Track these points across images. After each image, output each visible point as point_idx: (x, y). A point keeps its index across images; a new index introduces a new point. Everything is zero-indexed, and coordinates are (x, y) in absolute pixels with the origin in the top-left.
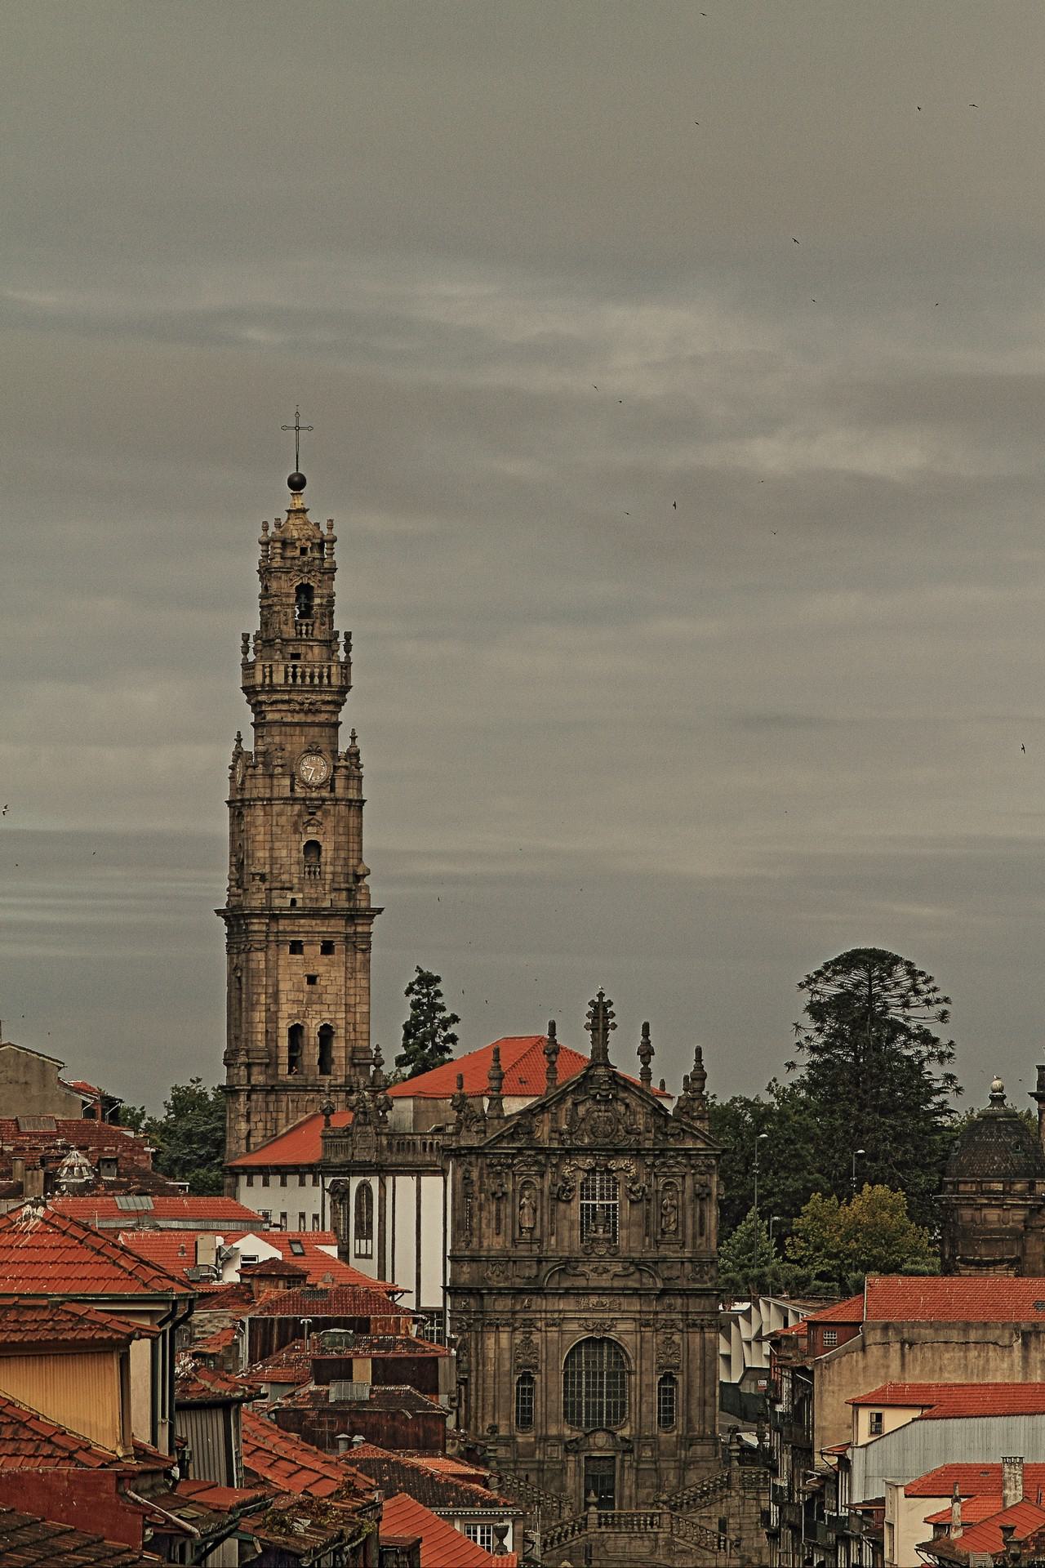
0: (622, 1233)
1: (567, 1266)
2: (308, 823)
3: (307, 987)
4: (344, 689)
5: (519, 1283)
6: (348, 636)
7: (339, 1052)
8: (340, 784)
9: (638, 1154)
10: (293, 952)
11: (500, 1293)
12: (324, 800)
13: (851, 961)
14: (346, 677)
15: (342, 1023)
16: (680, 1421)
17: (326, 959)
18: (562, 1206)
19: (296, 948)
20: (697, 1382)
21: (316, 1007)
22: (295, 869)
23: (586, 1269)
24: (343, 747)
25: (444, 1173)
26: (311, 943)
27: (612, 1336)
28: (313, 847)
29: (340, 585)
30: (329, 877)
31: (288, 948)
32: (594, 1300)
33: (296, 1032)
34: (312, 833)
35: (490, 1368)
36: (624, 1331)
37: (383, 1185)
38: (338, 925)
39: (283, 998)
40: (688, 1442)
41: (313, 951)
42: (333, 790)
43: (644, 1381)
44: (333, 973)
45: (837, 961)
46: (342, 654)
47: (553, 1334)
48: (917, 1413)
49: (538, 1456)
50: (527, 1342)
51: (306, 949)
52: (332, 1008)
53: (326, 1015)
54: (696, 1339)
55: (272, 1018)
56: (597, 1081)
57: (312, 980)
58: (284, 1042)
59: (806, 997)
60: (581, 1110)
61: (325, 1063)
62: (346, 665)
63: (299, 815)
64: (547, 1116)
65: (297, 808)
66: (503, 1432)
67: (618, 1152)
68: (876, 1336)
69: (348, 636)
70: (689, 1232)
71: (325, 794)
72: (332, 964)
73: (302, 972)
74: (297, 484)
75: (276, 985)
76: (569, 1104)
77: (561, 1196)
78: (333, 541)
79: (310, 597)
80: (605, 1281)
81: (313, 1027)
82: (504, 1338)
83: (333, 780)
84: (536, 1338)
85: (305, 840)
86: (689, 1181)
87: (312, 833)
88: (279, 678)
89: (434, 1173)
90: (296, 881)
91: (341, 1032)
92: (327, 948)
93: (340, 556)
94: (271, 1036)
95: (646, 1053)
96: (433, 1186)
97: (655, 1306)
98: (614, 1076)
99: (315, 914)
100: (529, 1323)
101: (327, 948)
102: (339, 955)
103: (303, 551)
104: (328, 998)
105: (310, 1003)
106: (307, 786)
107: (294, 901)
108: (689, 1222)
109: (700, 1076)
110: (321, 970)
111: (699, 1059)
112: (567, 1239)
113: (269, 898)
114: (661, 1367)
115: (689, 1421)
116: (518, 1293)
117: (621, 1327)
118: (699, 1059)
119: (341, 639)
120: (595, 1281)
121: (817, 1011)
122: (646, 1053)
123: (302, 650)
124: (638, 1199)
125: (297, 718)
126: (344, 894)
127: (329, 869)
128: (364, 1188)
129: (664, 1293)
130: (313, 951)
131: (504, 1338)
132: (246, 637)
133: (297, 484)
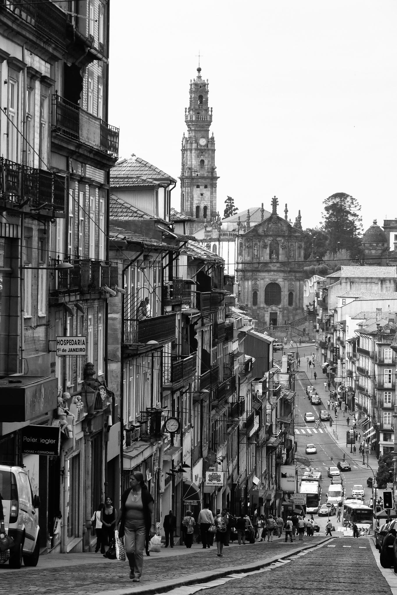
0: (280, 256)
1: (266, 264)
2: (201, 155)
4: (211, 121)
5: (254, 269)
6: (212, 108)
7: (209, 212)
8: (209, 145)
9: (284, 237)
10: (197, 187)
11: (249, 271)
12: (205, 149)
13: (335, 196)
14: (211, 119)
15: (209, 205)
16: (294, 304)
17: (205, 189)
18: (265, 250)
19: (198, 187)
20: (298, 294)
22: (198, 167)
23: (270, 265)
24: (210, 136)
25: (235, 241)
27: (277, 282)
28: (202, 162)
29: (209, 96)
32: (272, 273)
33: (198, 208)
34: (202, 158)
35: (246, 290)
36: (280, 281)
37: (219, 244)
38: (208, 181)
39: (195, 199)
40: (296, 309)
42: (207, 147)
43: (285, 293)
44: (207, 193)
45: (332, 196)
46: (210, 113)
47: (262, 282)
48: (354, 299)
49: (258, 312)
50: (256, 284)
54: (298, 283)
55: (192, 204)
56: (274, 218)
57: (202, 195)
58: (195, 210)
59: (325, 205)
60: (270, 225)
61: (205, 216)
62: (211, 116)
64: (261, 227)
66: (249, 306)
67: (279, 236)
68: (344, 281)
69: (212, 108)
70: (297, 256)
72: (207, 191)
74: (199, 70)
75: (193, 196)
76: (267, 224)
77: (265, 247)
78: (208, 84)
79: (202, 99)
80: (275, 268)
81: (202, 206)
82: (250, 282)
84: (258, 282)
86: (297, 244)
87: (202, 158)
88: (194, 119)
89: (233, 241)
91: (209, 208)
92: (206, 187)
93: (210, 88)
94: (191, 208)
95: (286, 211)
96: (232, 244)
97: (288, 275)
98: (278, 218)
99: (203, 178)
100: (256, 279)
102: (209, 189)
103: (201, 87)
104: (206, 199)
105: (201, 200)
106: (201, 146)
107: (197, 175)
108: (297, 253)
109: (300, 217)
110: (204, 192)
111: (299, 213)
112: (265, 257)
113: (191, 174)
114: (289, 290)
115: (296, 303)
116: (252, 271)
117: (279, 280)
118: (299, 213)
119: (210, 109)
120: (273, 268)
121: (327, 209)
122: (286, 211)
123: (200, 112)
124: (284, 248)
125: (199, 129)
126: (210, 173)
127: (206, 167)
128: (215, 246)
129: (290, 272)
131: (250, 282)
132: (186, 109)
133: (199, 70)
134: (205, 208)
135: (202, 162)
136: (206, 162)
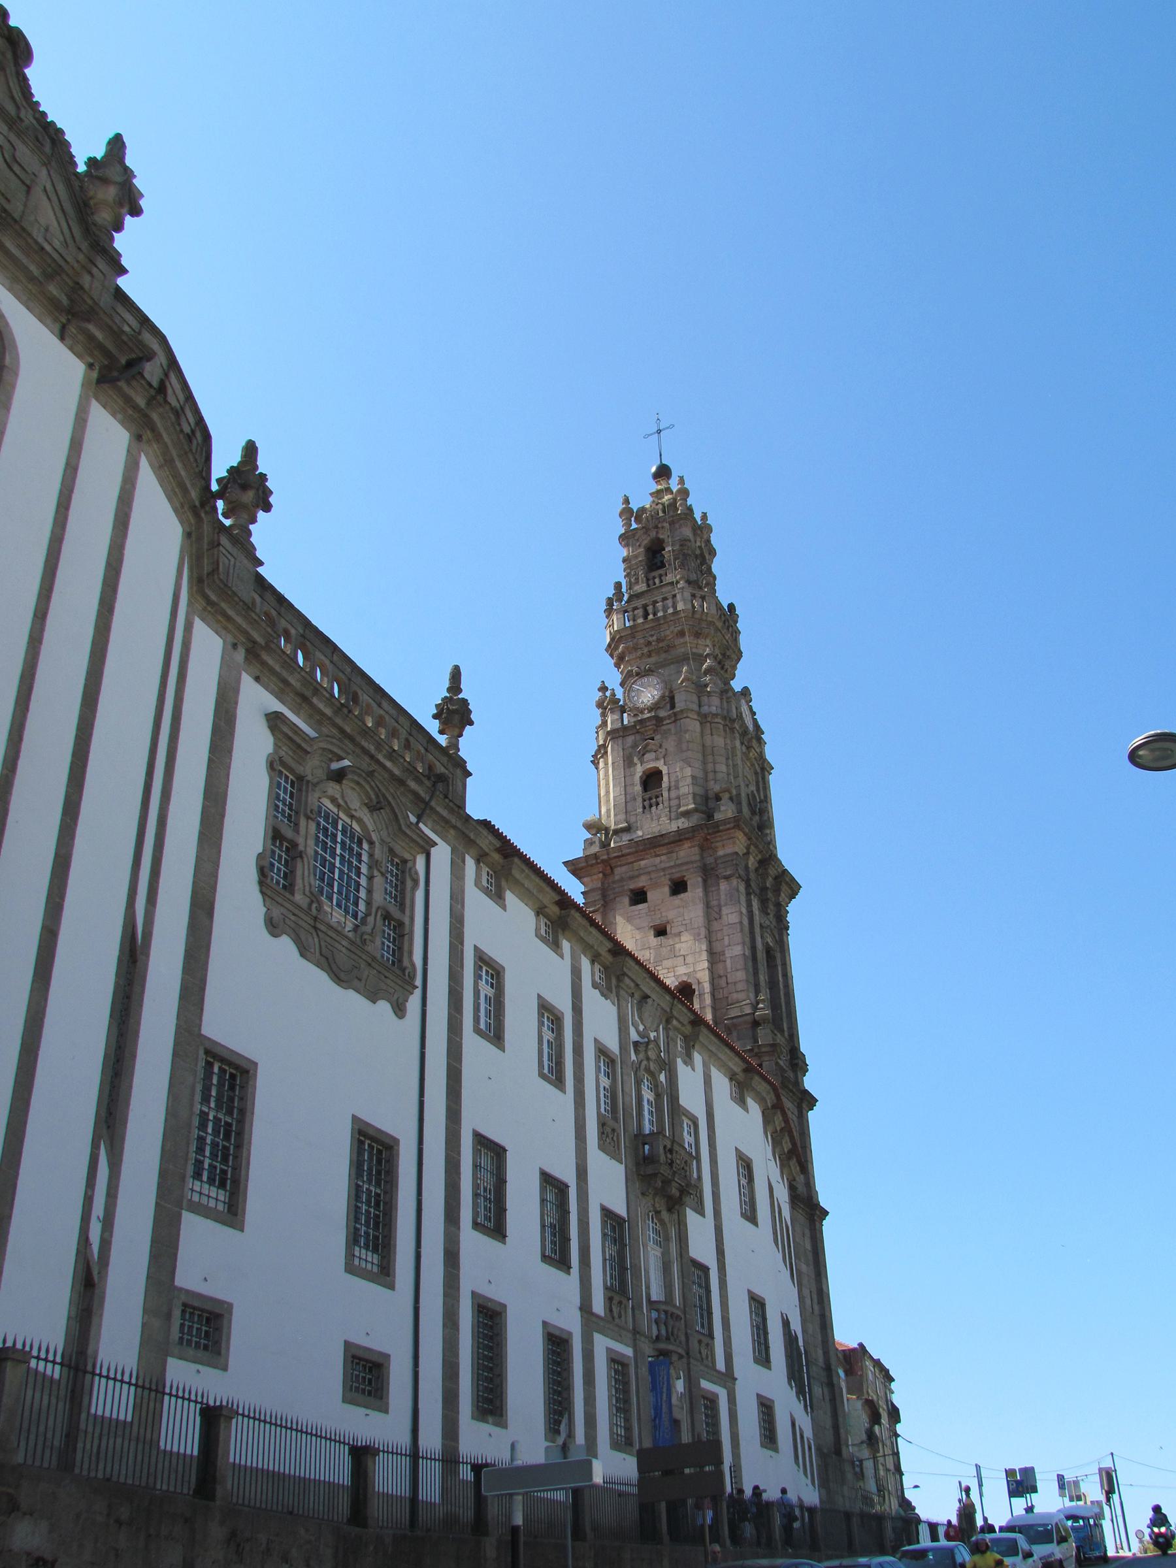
3: (653, 941)
15: (704, 976)
19: (639, 897)
21: (667, 963)
26: (656, 885)
28: (652, 780)
31: (626, 900)
38: (688, 852)
41: (659, 895)
42: (673, 706)
51: (649, 895)
52: (689, 959)
53: (682, 970)
63: (635, 746)
65: (630, 740)
71: (662, 713)
83: (672, 698)
85: (639, 770)
92: (678, 887)
102: (695, 892)
110: (671, 915)
130: (659, 895)
133: (663, 472)
135: (652, 780)
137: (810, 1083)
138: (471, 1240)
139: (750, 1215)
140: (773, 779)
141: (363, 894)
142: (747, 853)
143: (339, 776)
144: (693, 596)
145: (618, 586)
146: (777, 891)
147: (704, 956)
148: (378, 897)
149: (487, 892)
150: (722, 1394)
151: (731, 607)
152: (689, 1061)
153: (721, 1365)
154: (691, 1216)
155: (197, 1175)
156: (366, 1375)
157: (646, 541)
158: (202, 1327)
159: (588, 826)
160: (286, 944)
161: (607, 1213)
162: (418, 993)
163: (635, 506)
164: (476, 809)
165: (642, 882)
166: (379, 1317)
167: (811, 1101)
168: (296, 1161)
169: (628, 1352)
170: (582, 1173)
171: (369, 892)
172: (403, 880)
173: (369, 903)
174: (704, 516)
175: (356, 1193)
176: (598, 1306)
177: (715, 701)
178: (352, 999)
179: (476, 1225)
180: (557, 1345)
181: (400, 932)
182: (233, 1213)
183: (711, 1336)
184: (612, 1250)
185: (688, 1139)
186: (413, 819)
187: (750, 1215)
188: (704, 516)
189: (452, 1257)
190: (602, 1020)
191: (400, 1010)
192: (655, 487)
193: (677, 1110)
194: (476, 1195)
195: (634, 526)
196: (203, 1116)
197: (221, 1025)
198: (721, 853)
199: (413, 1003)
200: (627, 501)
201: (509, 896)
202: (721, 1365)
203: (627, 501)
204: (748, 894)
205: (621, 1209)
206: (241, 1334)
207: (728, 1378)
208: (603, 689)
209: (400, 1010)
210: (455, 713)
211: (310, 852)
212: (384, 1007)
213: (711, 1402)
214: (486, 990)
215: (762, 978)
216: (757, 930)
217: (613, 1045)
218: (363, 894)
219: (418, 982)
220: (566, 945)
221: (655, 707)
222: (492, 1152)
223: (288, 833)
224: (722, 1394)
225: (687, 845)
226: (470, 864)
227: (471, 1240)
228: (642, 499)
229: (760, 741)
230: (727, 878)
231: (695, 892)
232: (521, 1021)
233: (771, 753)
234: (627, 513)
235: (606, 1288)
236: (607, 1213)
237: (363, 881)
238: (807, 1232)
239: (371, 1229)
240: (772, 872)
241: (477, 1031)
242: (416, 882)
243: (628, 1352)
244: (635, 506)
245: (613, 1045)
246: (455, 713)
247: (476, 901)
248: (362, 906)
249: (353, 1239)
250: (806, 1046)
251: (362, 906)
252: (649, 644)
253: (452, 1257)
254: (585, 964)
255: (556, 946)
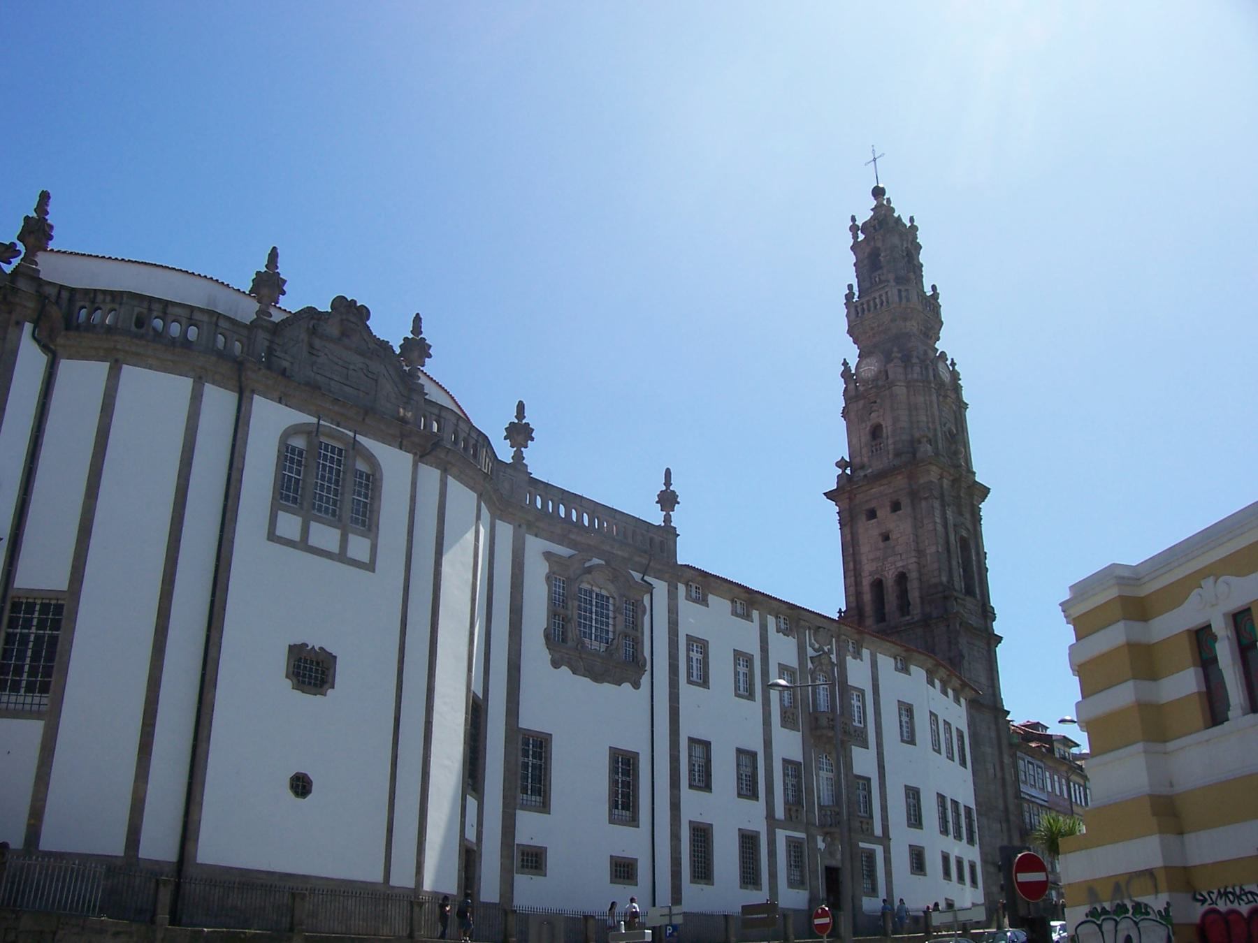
3: (881, 545)
7: (914, 595)
15: (913, 567)
17: (895, 516)
19: (872, 514)
28: (876, 432)
30: (891, 447)
31: (864, 517)
33: (878, 585)
38: (900, 481)
39: (864, 559)
42: (887, 377)
51: (878, 513)
53: (899, 564)
57: (886, 538)
58: (867, 597)
61: (904, 606)
65: (862, 402)
73: (875, 533)
85: (869, 424)
90: (865, 460)
91: (913, 575)
92: (896, 507)
101: (896, 507)
102: (906, 509)
127: (890, 441)
134: (902, 578)
135: (876, 432)
136: (888, 429)
137: (998, 628)
138: (689, 797)
139: (909, 738)
140: (969, 414)
141: (611, 628)
142: (942, 477)
143: (589, 570)
144: (900, 291)
145: (850, 287)
146: (971, 495)
147: (913, 554)
148: (620, 627)
149: (696, 601)
150: (879, 850)
151: (934, 288)
152: (857, 655)
153: (878, 831)
154: (856, 751)
155: (525, 790)
156: (623, 870)
157: (868, 250)
158: (534, 860)
159: (838, 465)
160: (565, 669)
161: (786, 762)
162: (647, 674)
163: (859, 223)
164: (681, 560)
165: (873, 504)
166: (631, 842)
167: (999, 639)
168: (579, 778)
169: (803, 835)
170: (768, 743)
171: (614, 625)
172: (635, 612)
173: (614, 632)
174: (912, 219)
175: (614, 783)
176: (780, 813)
177: (917, 369)
178: (607, 687)
179: (691, 786)
180: (748, 842)
181: (637, 643)
182: (545, 807)
183: (871, 817)
184: (791, 781)
185: (855, 702)
186: (637, 576)
187: (909, 738)
188: (912, 219)
189: (675, 806)
190: (784, 649)
191: (636, 685)
192: (874, 203)
193: (845, 688)
194: (691, 771)
195: (861, 237)
196: (525, 766)
197: (527, 721)
198: (921, 481)
199: (645, 679)
200: (853, 219)
201: (712, 598)
202: (878, 831)
203: (853, 219)
204: (943, 506)
205: (797, 756)
206: (551, 860)
207: (885, 839)
208: (845, 363)
209: (636, 685)
210: (668, 500)
211: (575, 617)
212: (627, 686)
213: (871, 856)
214: (695, 655)
215: (954, 563)
216: (951, 530)
217: (794, 663)
218: (611, 628)
219: (648, 667)
220: (755, 614)
221: (876, 379)
222: (702, 747)
223: (561, 611)
224: (879, 850)
225: (899, 477)
226: (682, 588)
227: (689, 797)
228: (864, 216)
229: (957, 389)
230: (926, 499)
231: (906, 509)
232: (722, 669)
233: (966, 396)
234: (854, 229)
235: (786, 802)
236: (786, 762)
237: (611, 621)
238: (993, 726)
239: (623, 801)
240: (963, 485)
241: (690, 682)
242: (644, 612)
243: (803, 835)
244: (859, 223)
245: (794, 663)
246: (668, 500)
247: (686, 608)
248: (611, 635)
249: (614, 805)
250: (994, 601)
251: (611, 635)
252: (872, 329)
253: (675, 806)
254: (771, 620)
255: (747, 616)
